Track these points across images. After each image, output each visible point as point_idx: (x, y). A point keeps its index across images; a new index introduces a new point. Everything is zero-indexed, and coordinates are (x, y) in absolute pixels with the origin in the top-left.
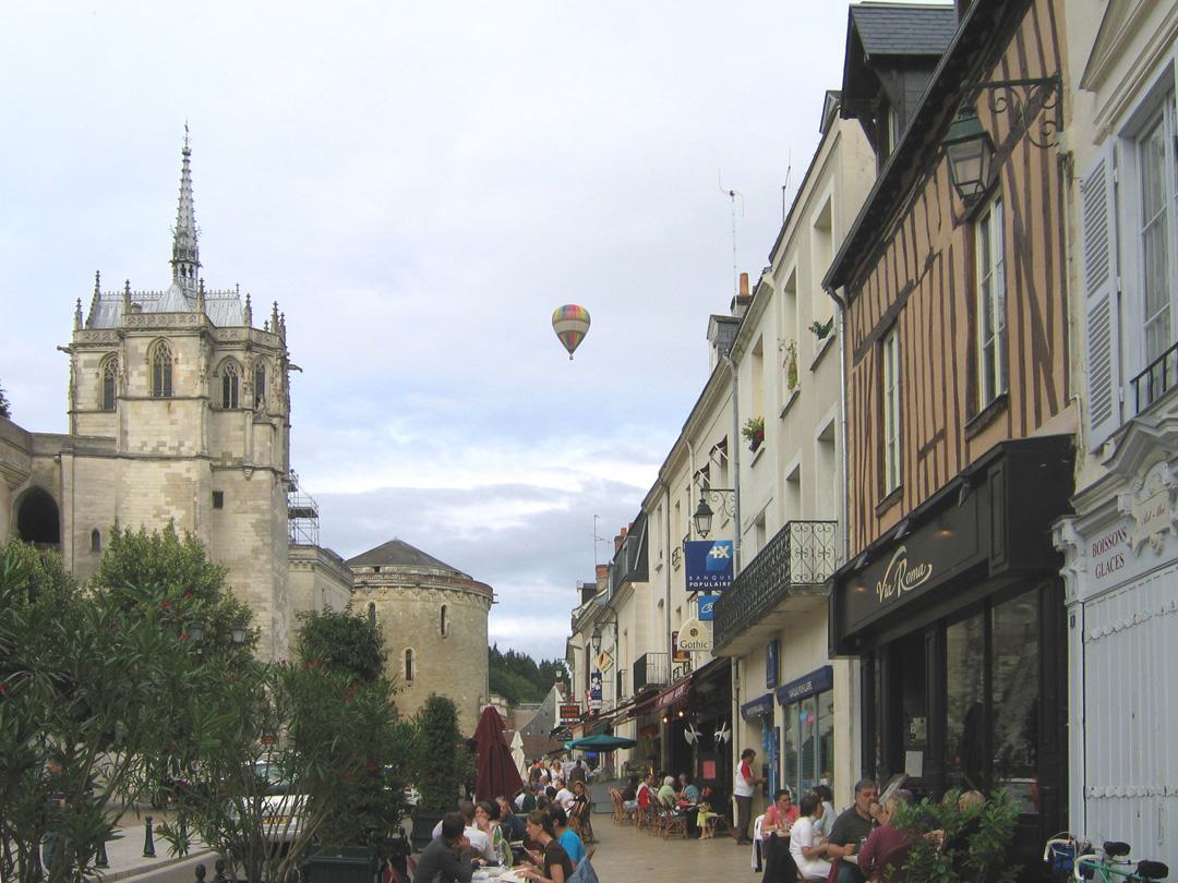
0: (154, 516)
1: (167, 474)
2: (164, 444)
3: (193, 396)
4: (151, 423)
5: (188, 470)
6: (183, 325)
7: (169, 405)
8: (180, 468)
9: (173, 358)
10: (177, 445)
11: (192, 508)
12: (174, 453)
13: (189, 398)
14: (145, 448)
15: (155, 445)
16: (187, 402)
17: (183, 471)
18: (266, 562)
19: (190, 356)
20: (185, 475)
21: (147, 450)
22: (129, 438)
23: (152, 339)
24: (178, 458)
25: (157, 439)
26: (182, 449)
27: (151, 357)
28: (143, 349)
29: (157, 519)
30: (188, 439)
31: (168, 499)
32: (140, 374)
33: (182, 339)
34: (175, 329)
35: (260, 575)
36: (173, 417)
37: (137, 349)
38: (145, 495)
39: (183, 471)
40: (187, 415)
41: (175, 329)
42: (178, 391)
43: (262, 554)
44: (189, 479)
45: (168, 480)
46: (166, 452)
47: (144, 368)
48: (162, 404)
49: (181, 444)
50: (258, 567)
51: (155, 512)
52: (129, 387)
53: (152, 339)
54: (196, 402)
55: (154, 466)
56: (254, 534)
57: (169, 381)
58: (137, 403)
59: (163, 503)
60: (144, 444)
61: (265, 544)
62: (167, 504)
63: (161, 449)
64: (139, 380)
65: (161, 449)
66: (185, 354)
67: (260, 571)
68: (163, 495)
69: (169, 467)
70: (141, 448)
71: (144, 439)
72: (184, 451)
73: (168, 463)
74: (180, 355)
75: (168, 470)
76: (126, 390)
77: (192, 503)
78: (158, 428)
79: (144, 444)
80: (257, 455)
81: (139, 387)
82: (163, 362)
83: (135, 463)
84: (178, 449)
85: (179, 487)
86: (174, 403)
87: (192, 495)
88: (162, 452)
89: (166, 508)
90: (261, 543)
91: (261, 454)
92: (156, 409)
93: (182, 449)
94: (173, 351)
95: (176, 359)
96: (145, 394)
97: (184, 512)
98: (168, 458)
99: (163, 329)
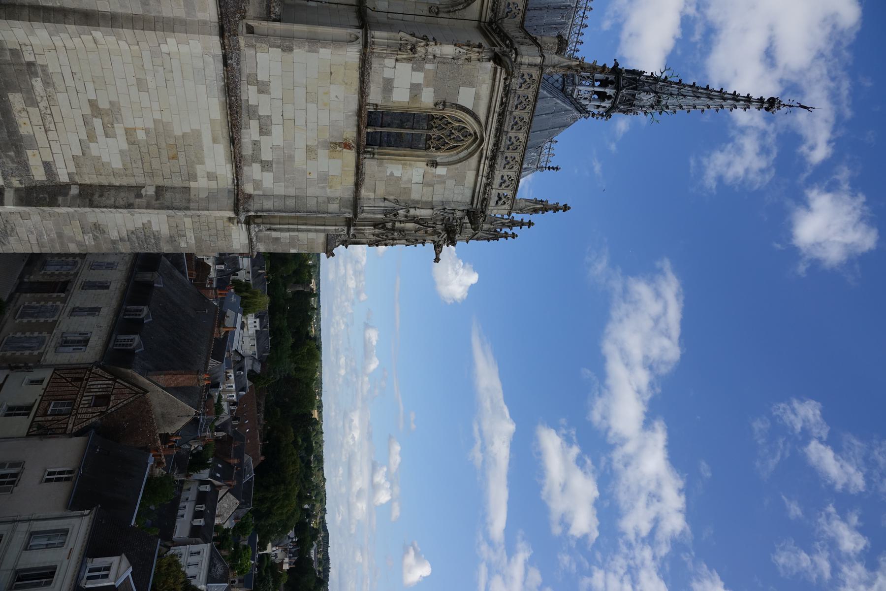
0: (93, 104)
1: (197, 134)
2: (264, 130)
3: (364, 193)
4: (311, 107)
5: (211, 176)
6: (497, 181)
7: (347, 146)
8: (216, 163)
9: (441, 156)
10: (266, 156)
11: (132, 181)
12: (247, 150)
13: (358, 185)
14: (253, 89)
15: (262, 112)
16: (351, 179)
17: (209, 165)
18: (79, 244)
19: (437, 187)
20: (200, 170)
21: (250, 94)
22: (276, 52)
23: (483, 119)
24: (237, 161)
25: (276, 119)
26: (256, 167)
27: (449, 112)
28: (466, 97)
29: (87, 111)
30: (276, 180)
31: (141, 135)
32: (415, 89)
33: (470, 176)
34: (492, 168)
35: (53, 235)
36: (323, 153)
37: (471, 84)
38: (141, 85)
39: (209, 165)
40: (324, 178)
41: (492, 168)
42: (370, 166)
43: (95, 238)
44: (193, 177)
45: (184, 135)
46: (250, 133)
47: (427, 99)
48: (350, 133)
49: (266, 166)
50: (67, 231)
51: (103, 105)
52: (389, 62)
53: (483, 119)
54: (349, 194)
55: (213, 108)
56: (131, 227)
57: (396, 142)
58: (356, 75)
59: (130, 125)
60: (263, 88)
61: (114, 242)
62: (129, 133)
63: (254, 124)
64: (403, 83)
65: (254, 124)
66: (442, 180)
67: (60, 235)
68: (150, 125)
69: (215, 141)
70: (253, 80)
71: (276, 90)
72: (253, 171)
73: (222, 132)
74: (441, 171)
75: (207, 139)
76: (380, 56)
77: (140, 180)
78: (300, 121)
79: (263, 88)
80: (274, 234)
81: (388, 86)
82: (435, 133)
83: (215, 68)
84: (256, 158)
85: (175, 157)
86: (350, 156)
87: (160, 182)
88: (248, 127)
89: (119, 129)
90: (114, 235)
91: (277, 240)
92: (339, 113)
93: (256, 167)
94: (452, 156)
95: (434, 164)
96: (375, 96)
97: (117, 164)
98: (234, 141)
99: (497, 144)
